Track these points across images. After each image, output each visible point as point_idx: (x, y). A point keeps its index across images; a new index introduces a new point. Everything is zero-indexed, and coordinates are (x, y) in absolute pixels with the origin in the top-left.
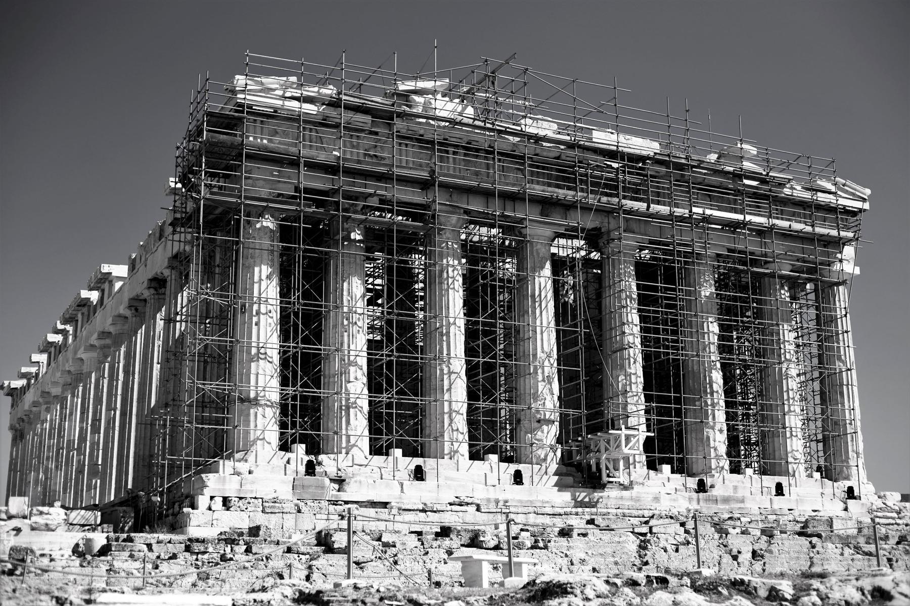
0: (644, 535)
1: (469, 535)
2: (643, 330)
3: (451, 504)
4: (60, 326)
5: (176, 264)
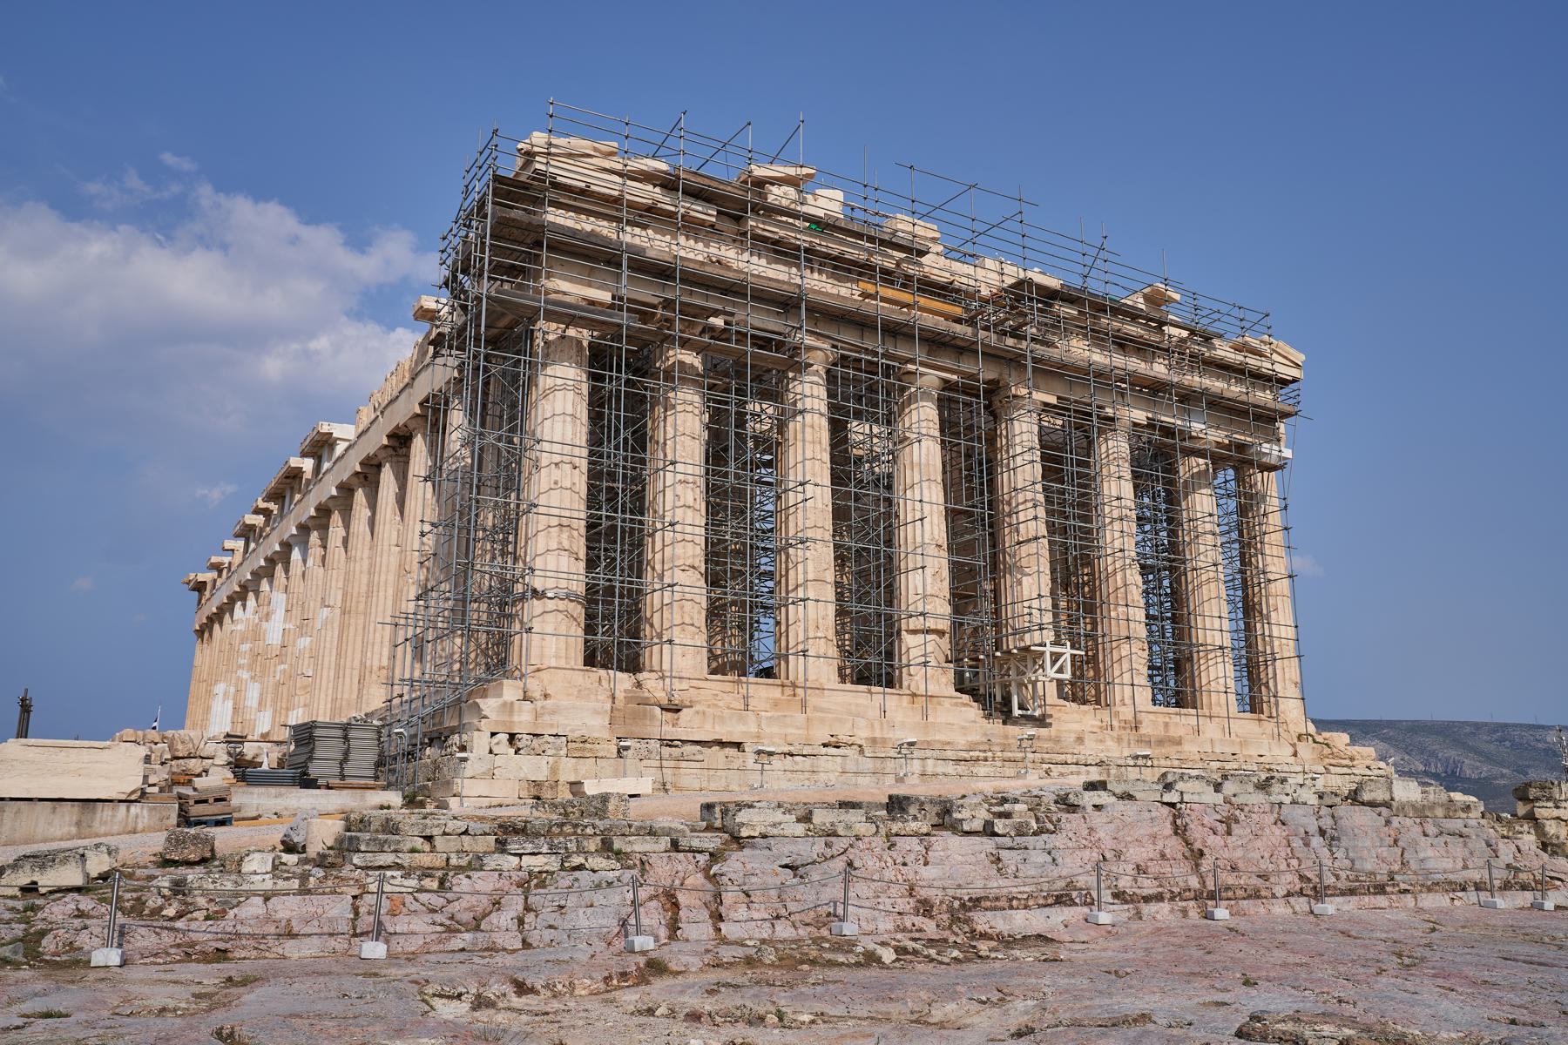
0: (1172, 805)
1: (937, 809)
2: (1049, 513)
3: (825, 745)
4: (262, 505)
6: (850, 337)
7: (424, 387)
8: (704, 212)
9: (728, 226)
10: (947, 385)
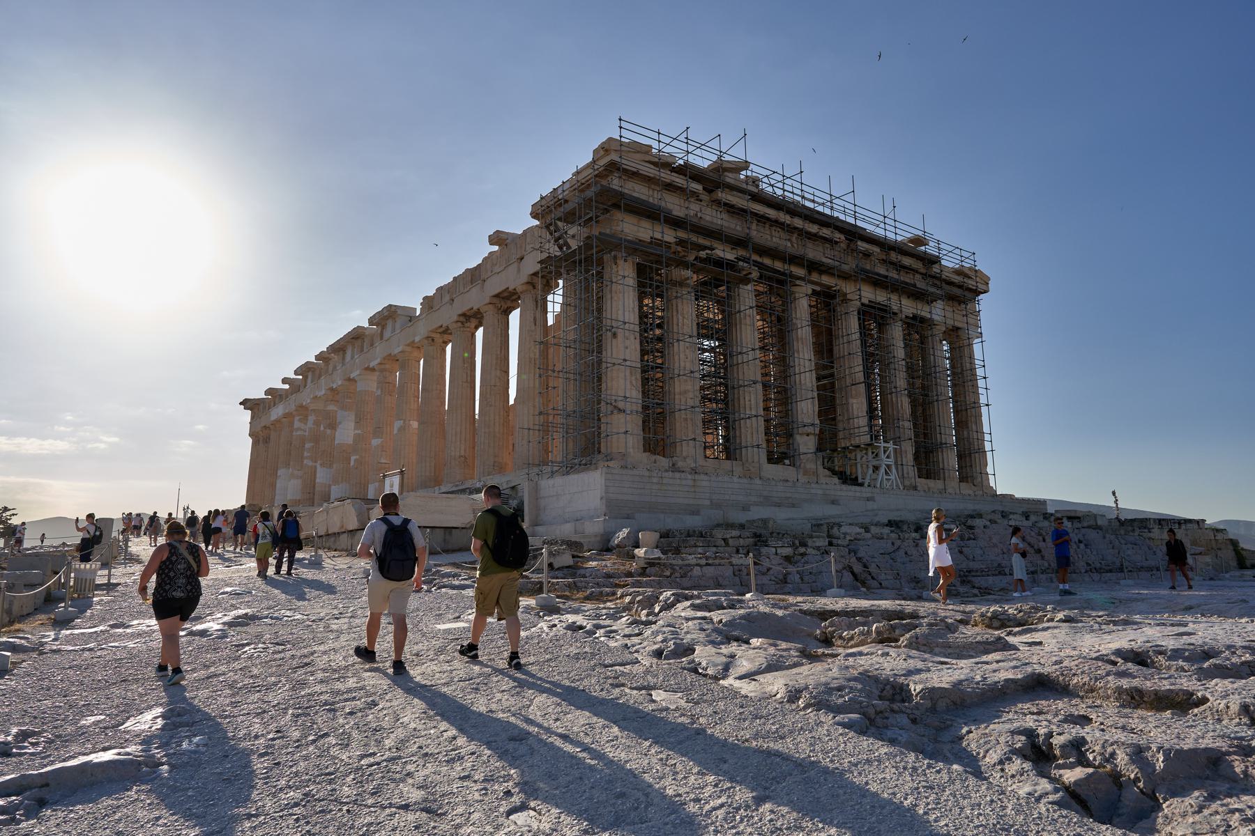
5: (495, 300)
6: (767, 261)
7: (496, 285)
8: (697, 187)
9: (705, 197)
10: (814, 292)
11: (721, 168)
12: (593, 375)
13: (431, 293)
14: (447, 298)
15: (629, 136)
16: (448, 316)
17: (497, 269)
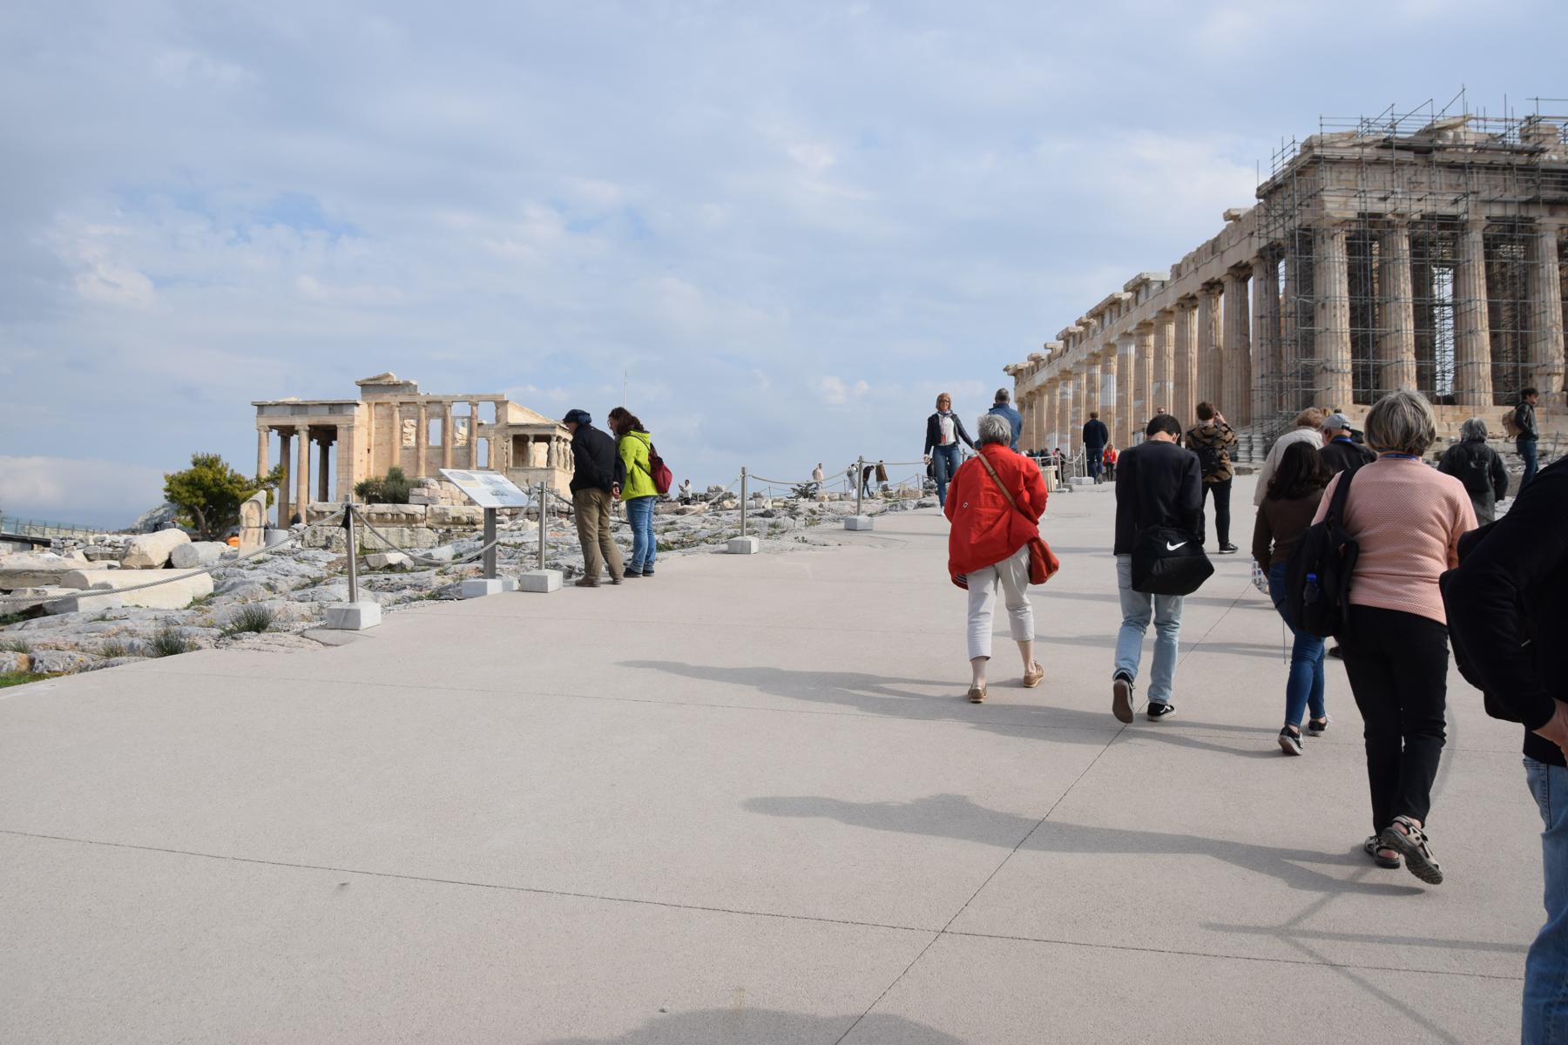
7: (1232, 258)
8: (1408, 156)
9: (1420, 160)
11: (1434, 131)
12: (1308, 344)
13: (1178, 261)
14: (1192, 268)
15: (1327, 131)
16: (1193, 285)
17: (1232, 243)
